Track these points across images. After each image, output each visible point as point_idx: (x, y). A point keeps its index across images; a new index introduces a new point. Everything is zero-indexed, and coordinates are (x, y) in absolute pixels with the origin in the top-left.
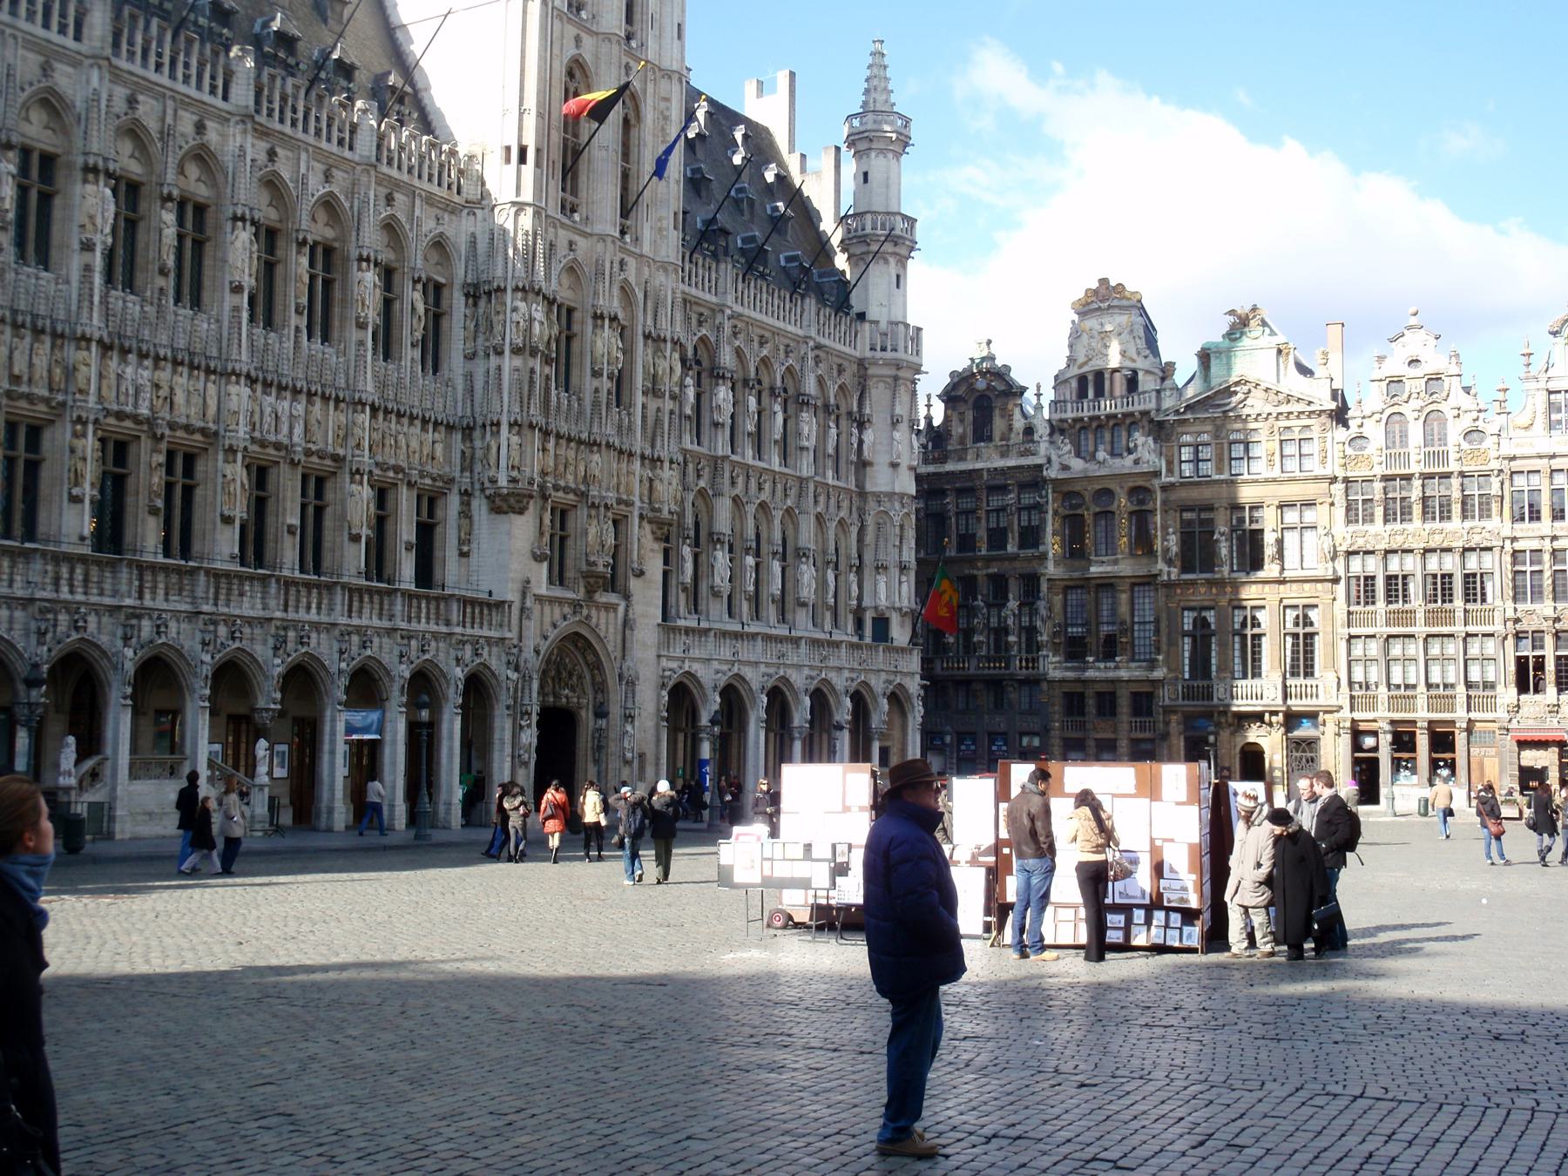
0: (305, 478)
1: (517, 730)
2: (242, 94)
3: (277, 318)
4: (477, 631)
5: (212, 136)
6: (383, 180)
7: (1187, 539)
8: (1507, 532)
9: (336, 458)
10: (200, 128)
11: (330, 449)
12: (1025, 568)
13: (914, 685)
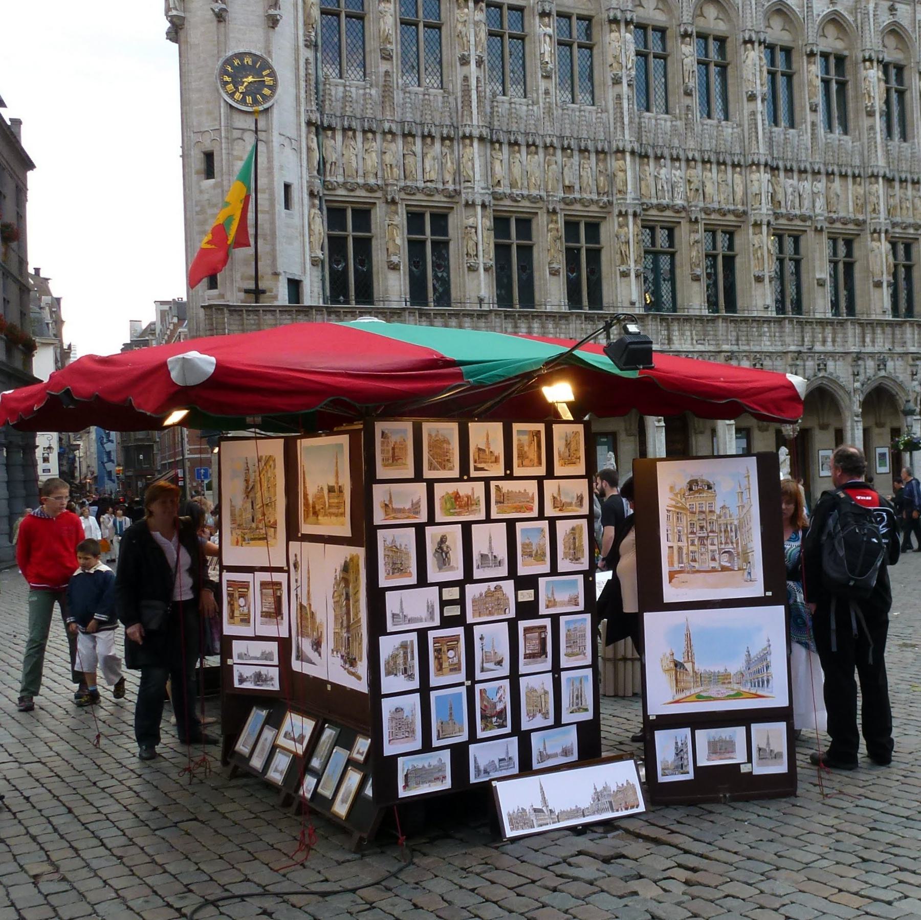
9: (858, 223)
11: (852, 216)
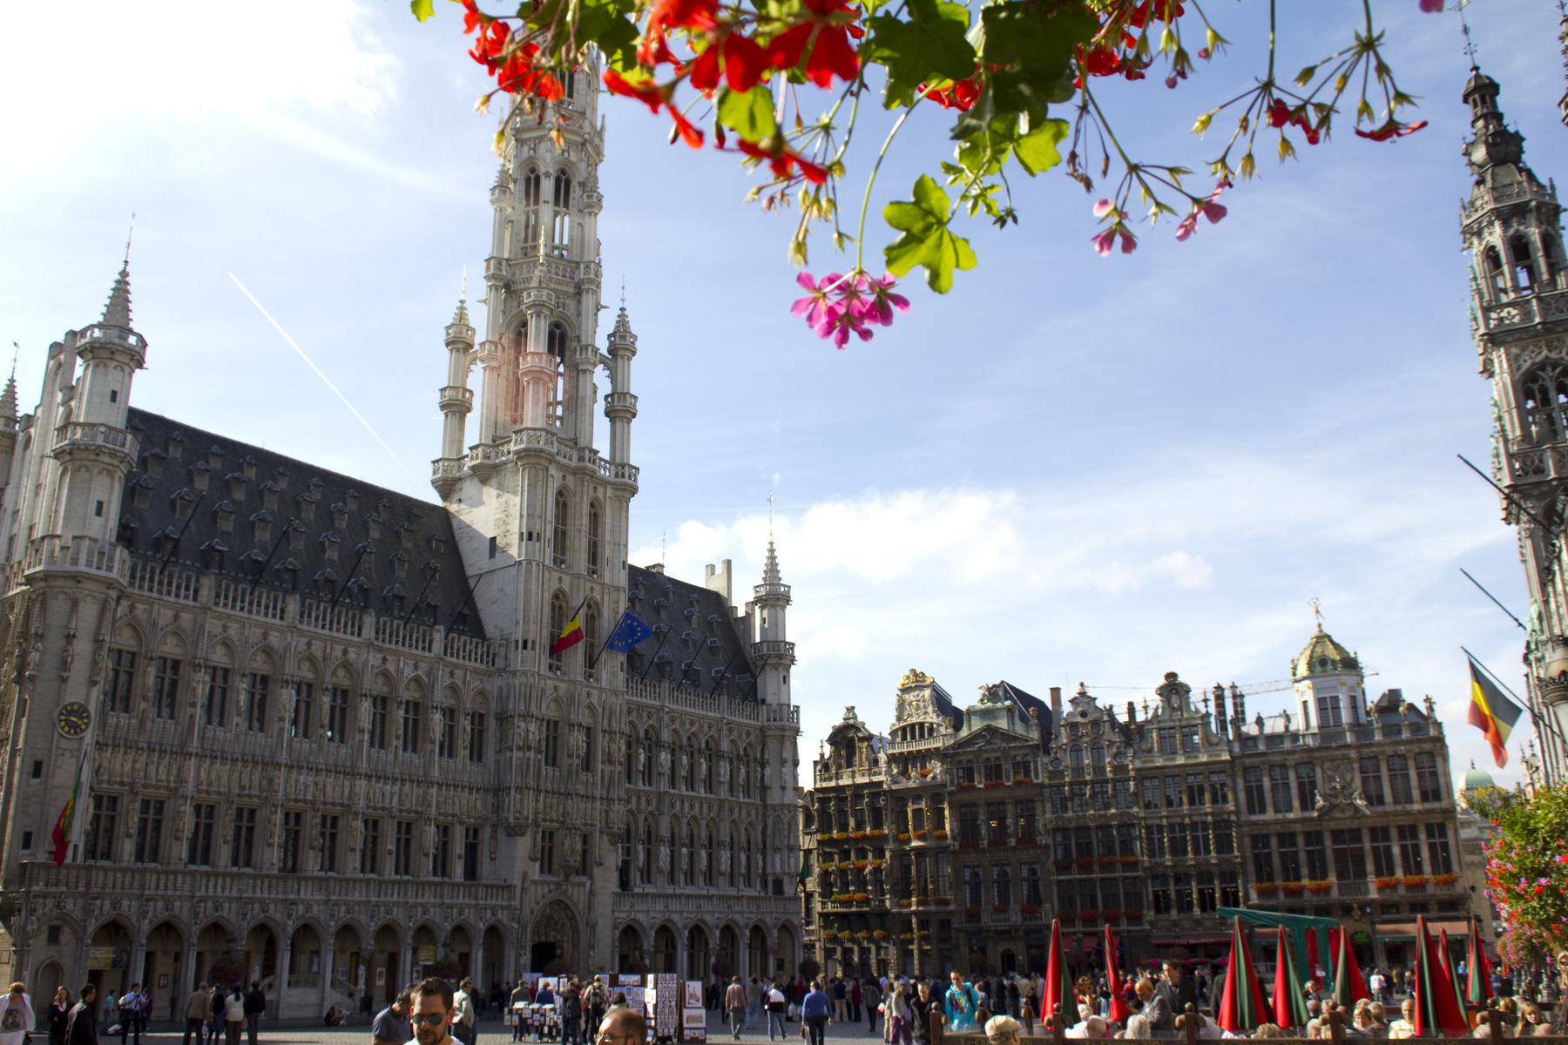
0: (400, 824)
1: (518, 956)
2: (368, 632)
4: (494, 902)
5: (352, 655)
6: (447, 664)
8: (1142, 815)
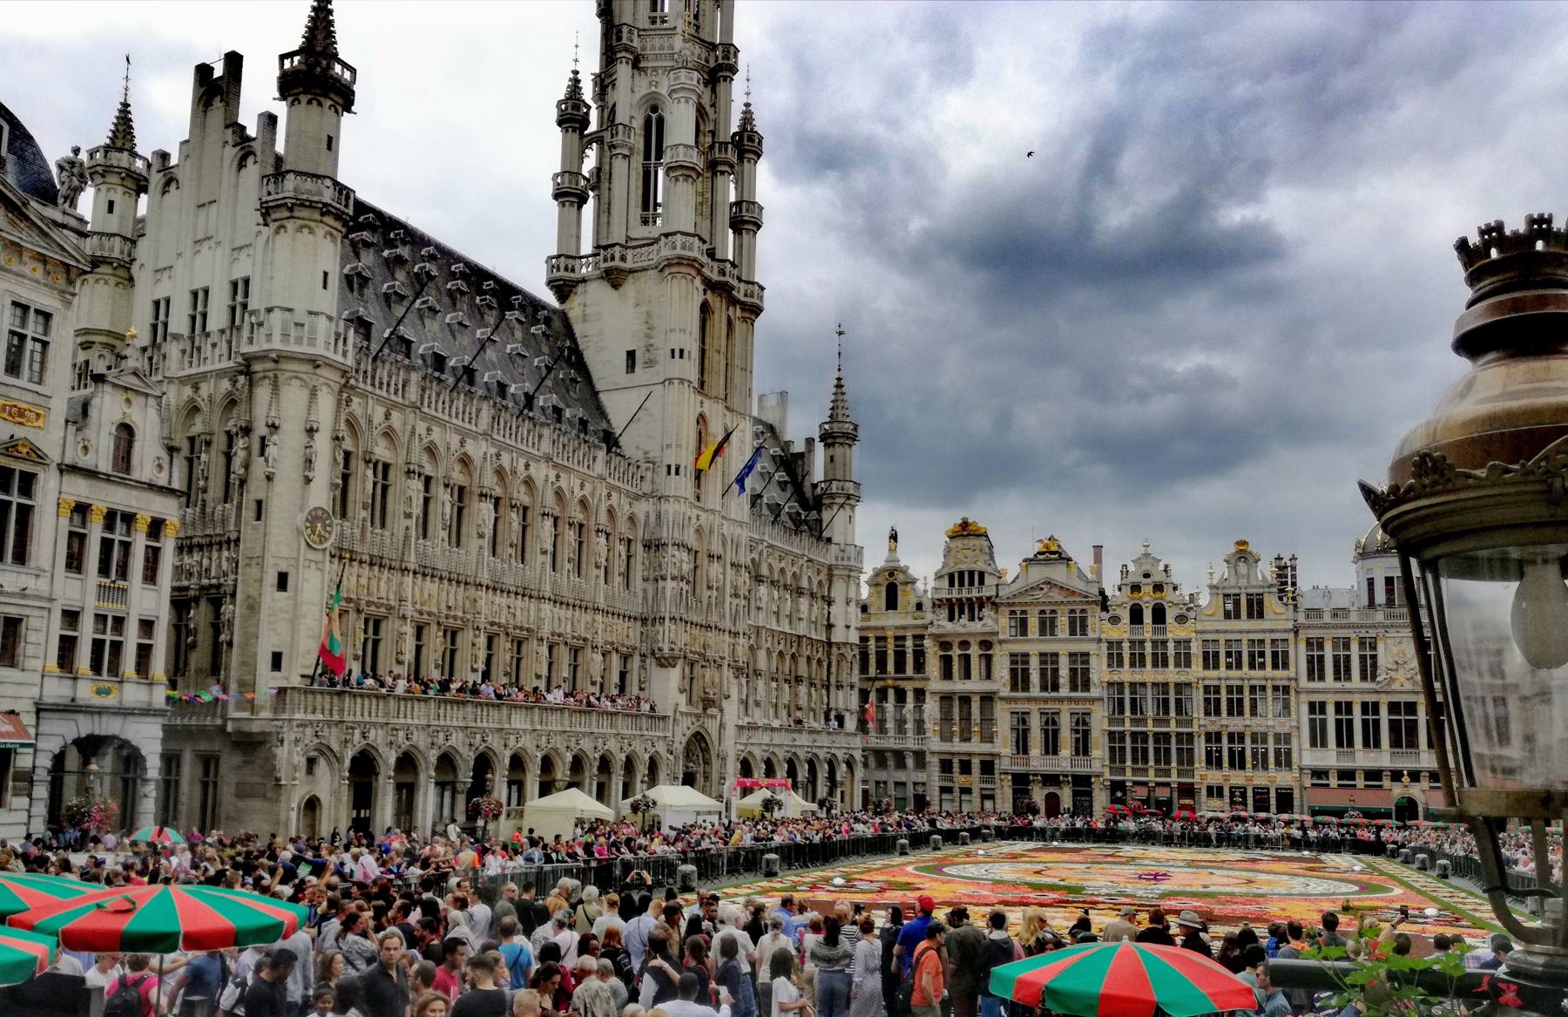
3: (558, 564)
5: (532, 470)
7: (1013, 672)
9: (585, 640)
10: (527, 466)
12: (918, 685)
13: (858, 755)
